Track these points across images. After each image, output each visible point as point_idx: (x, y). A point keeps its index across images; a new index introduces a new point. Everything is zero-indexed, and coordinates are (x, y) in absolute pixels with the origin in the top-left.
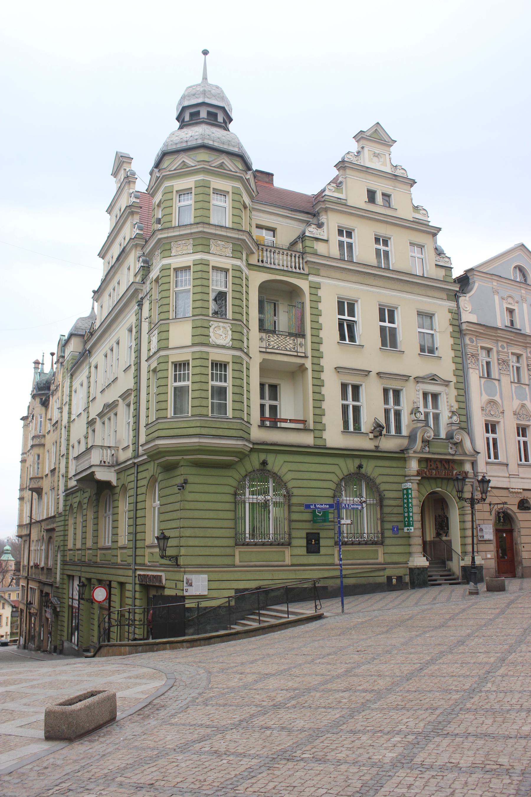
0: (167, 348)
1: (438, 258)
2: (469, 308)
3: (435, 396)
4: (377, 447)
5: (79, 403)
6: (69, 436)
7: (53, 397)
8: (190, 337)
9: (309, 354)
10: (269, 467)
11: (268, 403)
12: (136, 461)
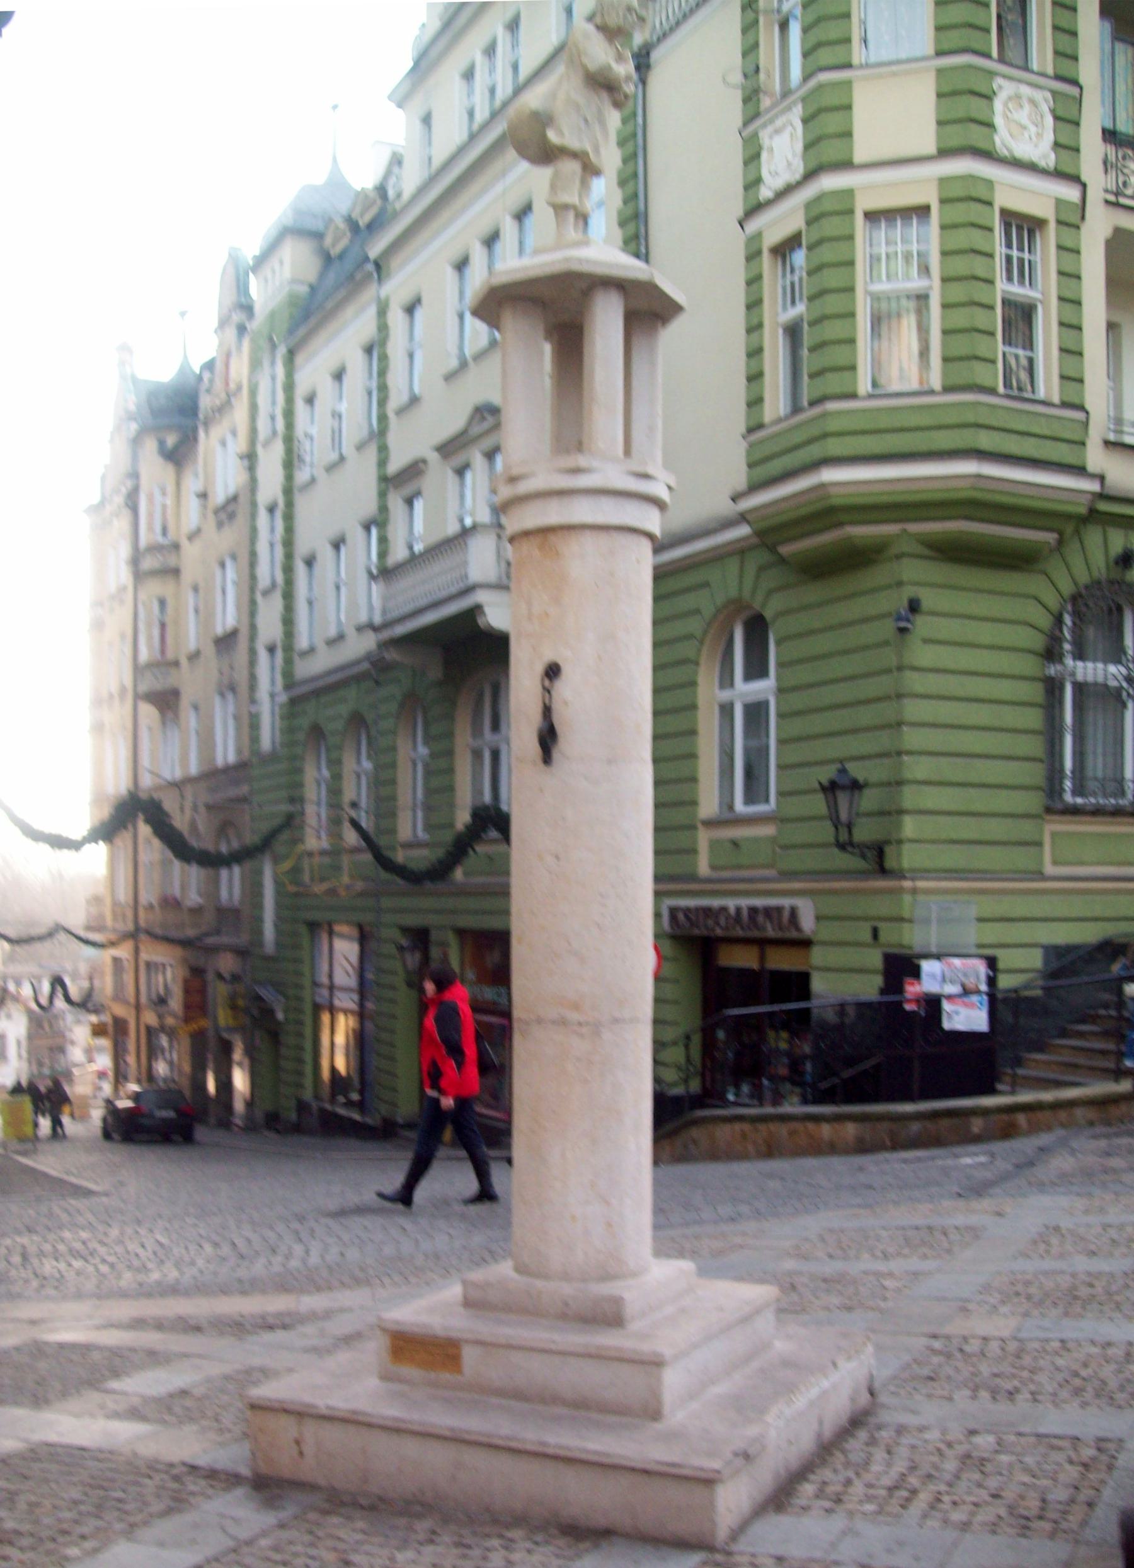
0: (846, 165)
6: (289, 530)
7: (207, 432)
8: (931, 127)
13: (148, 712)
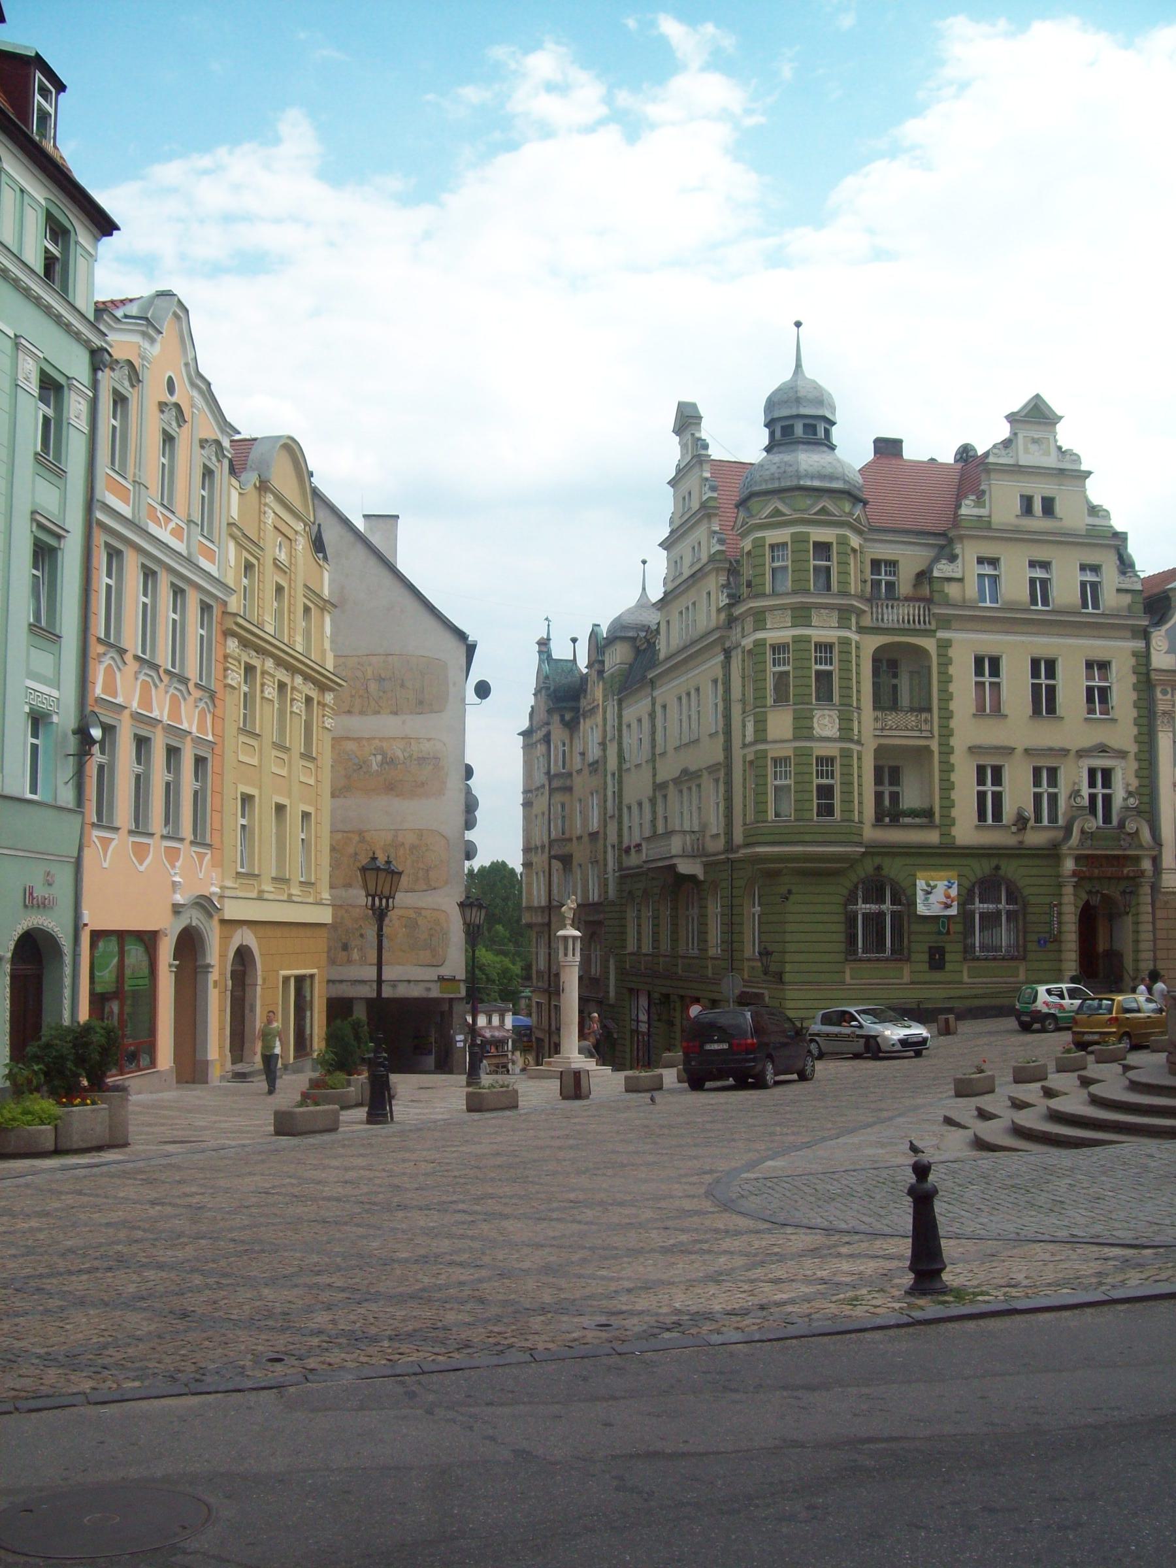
0: (765, 741)
1: (1122, 578)
2: (1165, 647)
3: (1107, 774)
4: (1021, 842)
5: (636, 751)
6: (620, 790)
9: (936, 733)
10: (885, 872)
11: (887, 789)
12: (731, 856)
13: (557, 865)
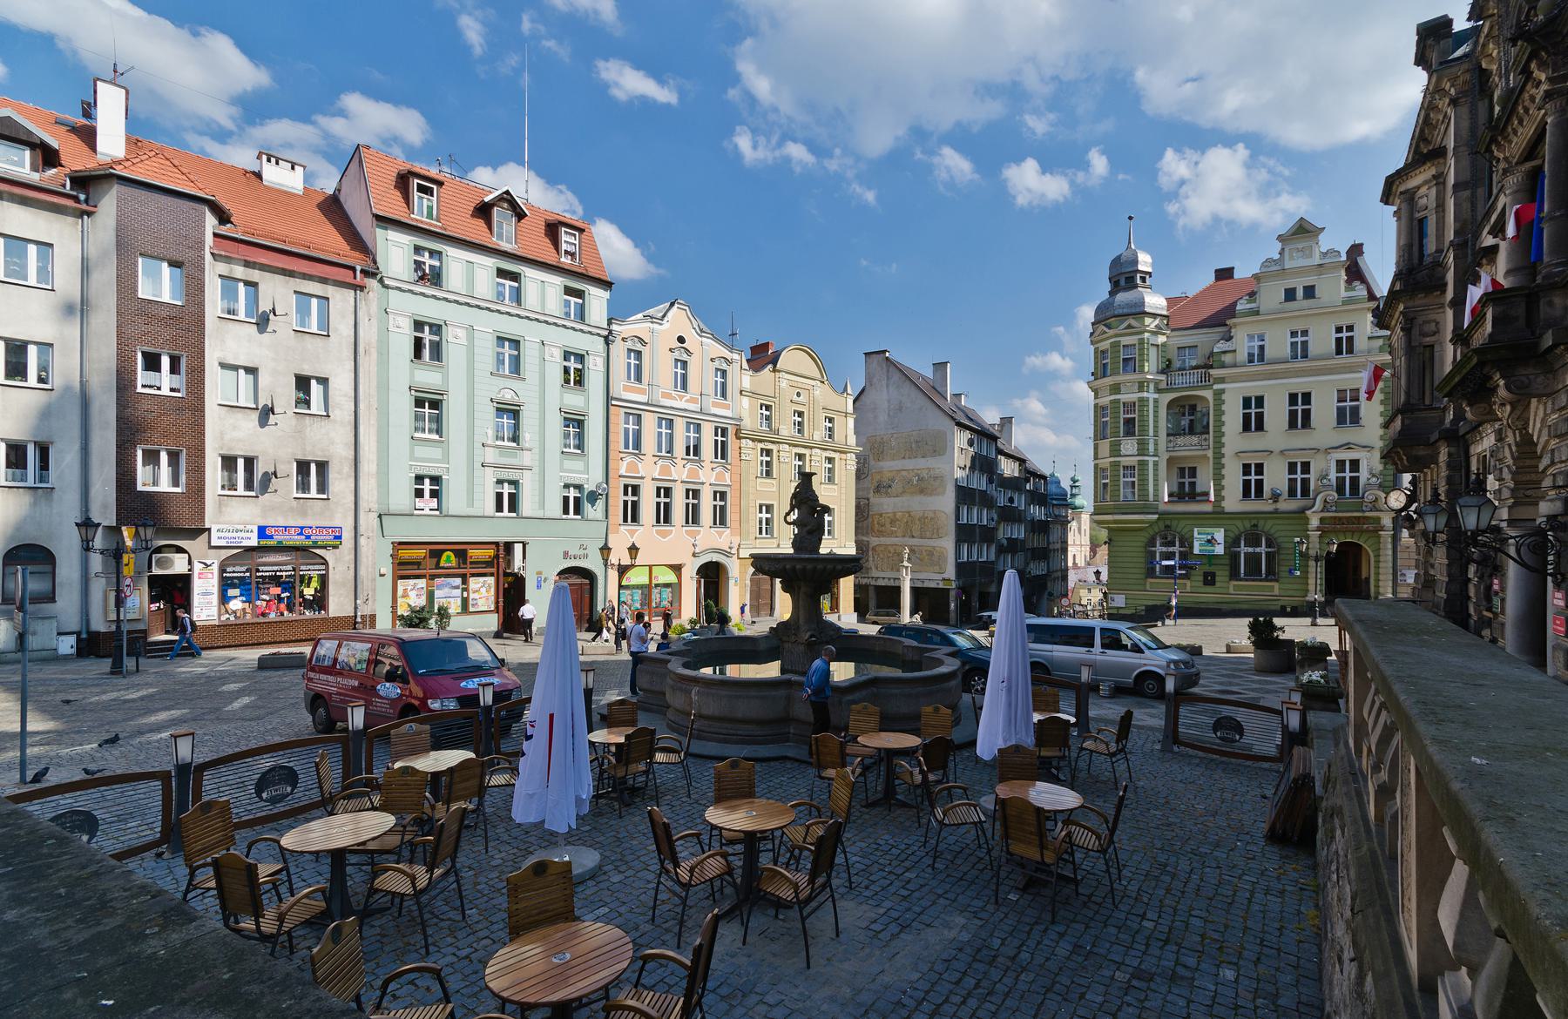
3: (1355, 465)
